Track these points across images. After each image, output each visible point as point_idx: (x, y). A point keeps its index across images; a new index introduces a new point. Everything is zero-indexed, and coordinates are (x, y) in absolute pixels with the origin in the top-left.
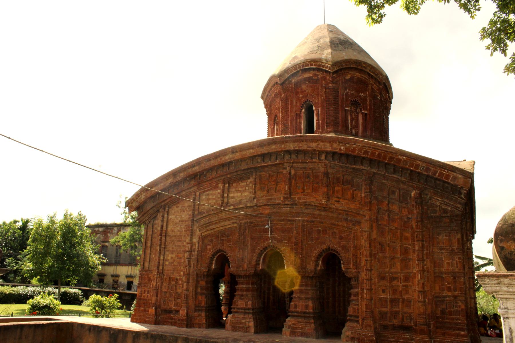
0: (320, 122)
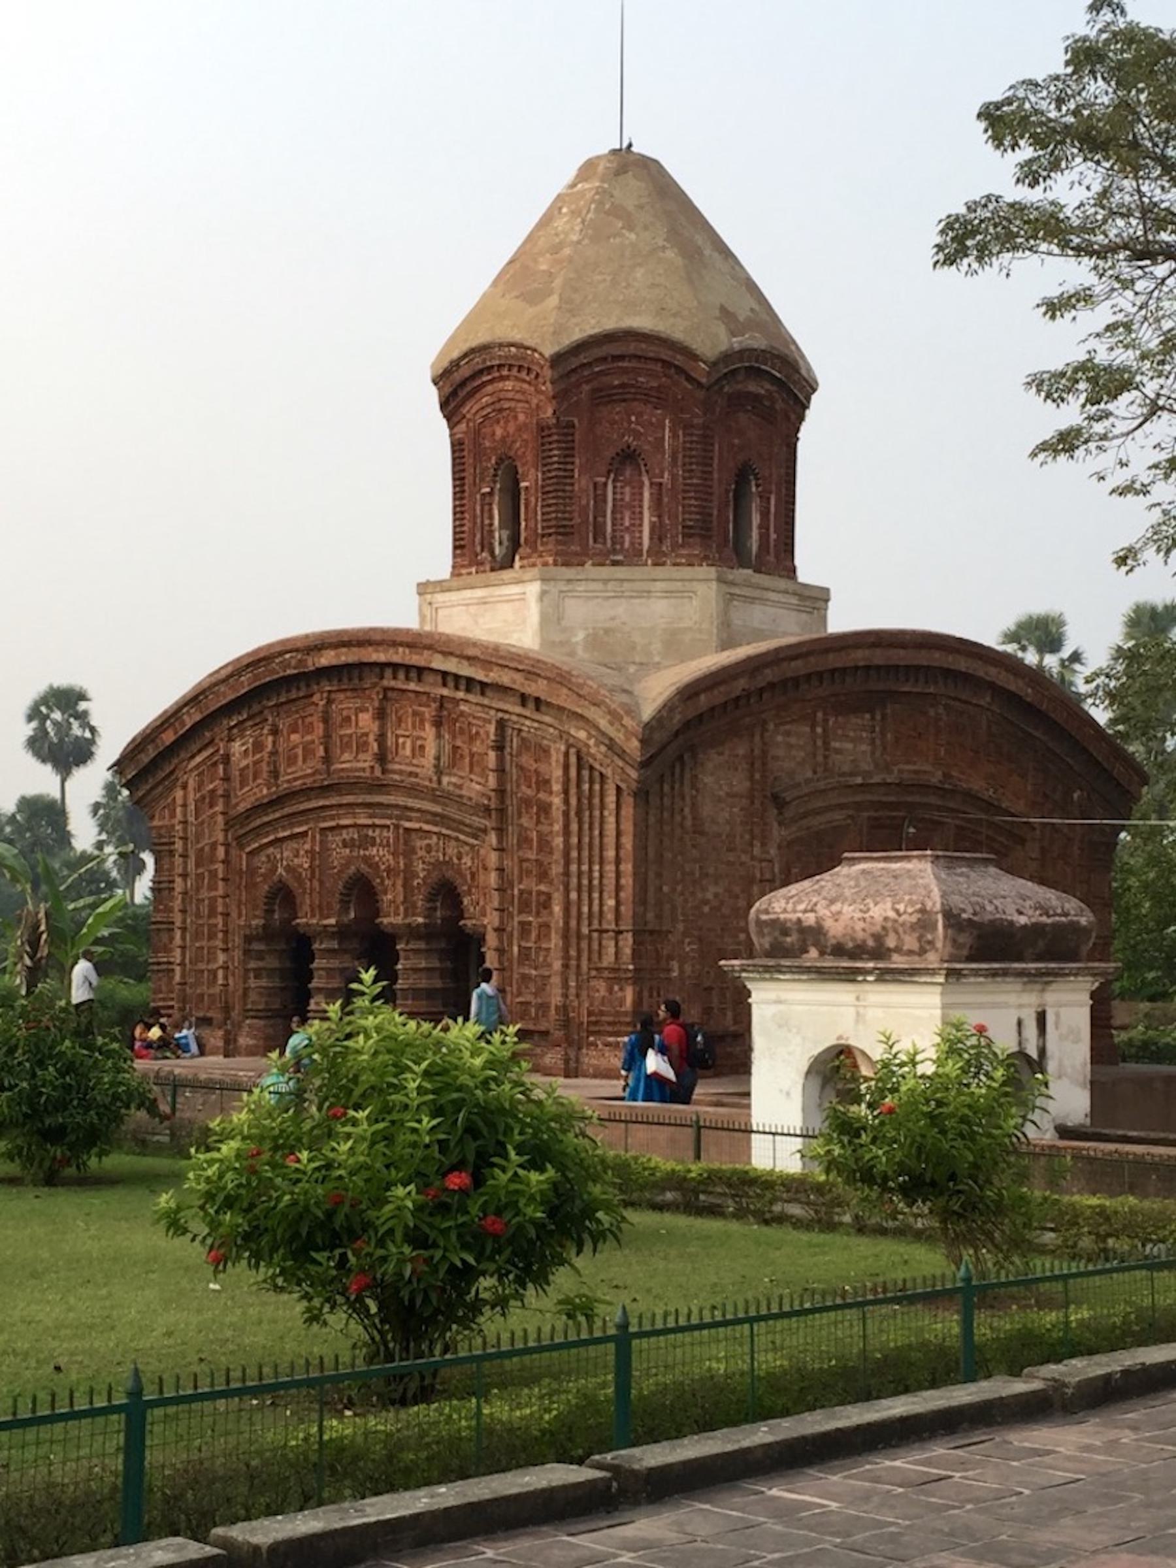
0: (773, 536)
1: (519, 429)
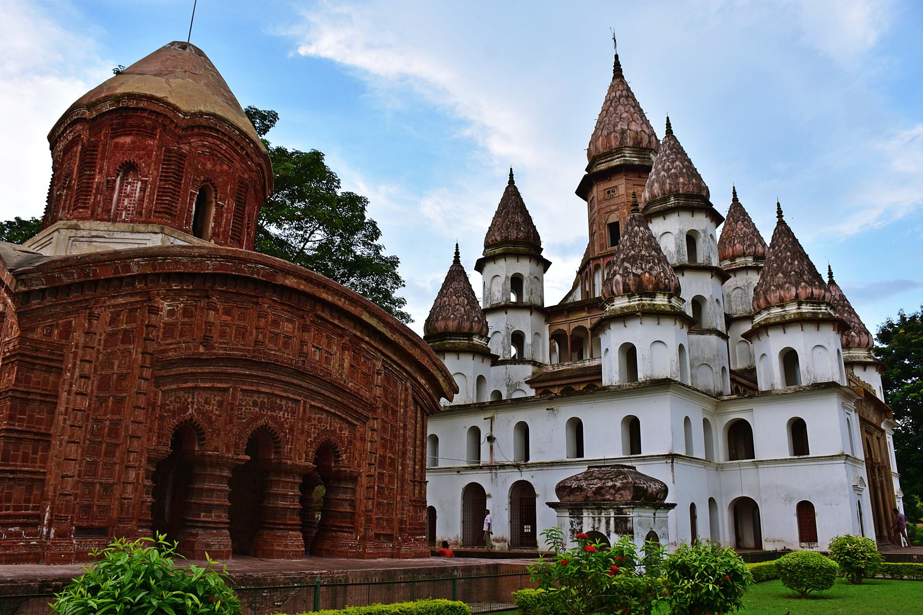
1: (222, 172)
